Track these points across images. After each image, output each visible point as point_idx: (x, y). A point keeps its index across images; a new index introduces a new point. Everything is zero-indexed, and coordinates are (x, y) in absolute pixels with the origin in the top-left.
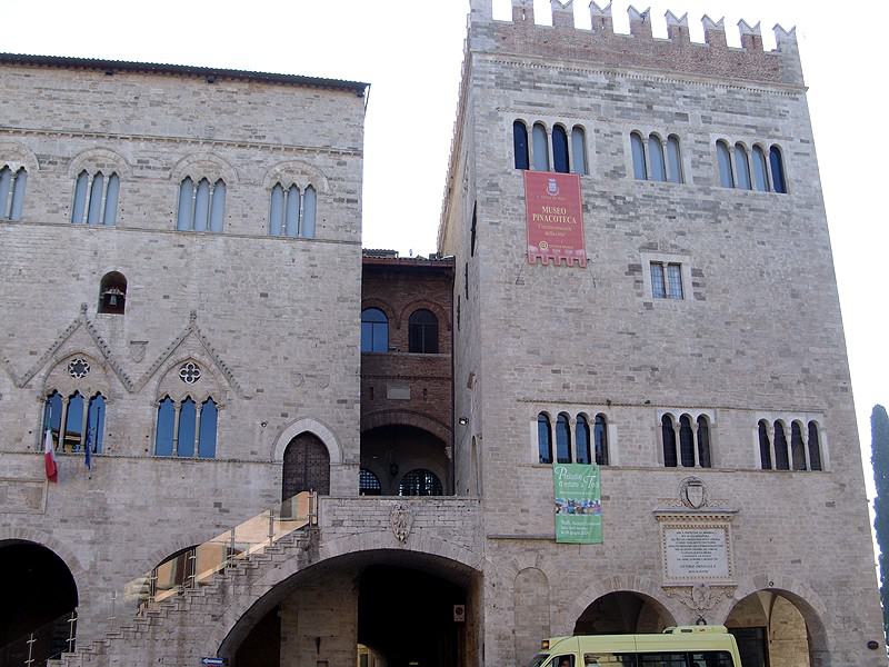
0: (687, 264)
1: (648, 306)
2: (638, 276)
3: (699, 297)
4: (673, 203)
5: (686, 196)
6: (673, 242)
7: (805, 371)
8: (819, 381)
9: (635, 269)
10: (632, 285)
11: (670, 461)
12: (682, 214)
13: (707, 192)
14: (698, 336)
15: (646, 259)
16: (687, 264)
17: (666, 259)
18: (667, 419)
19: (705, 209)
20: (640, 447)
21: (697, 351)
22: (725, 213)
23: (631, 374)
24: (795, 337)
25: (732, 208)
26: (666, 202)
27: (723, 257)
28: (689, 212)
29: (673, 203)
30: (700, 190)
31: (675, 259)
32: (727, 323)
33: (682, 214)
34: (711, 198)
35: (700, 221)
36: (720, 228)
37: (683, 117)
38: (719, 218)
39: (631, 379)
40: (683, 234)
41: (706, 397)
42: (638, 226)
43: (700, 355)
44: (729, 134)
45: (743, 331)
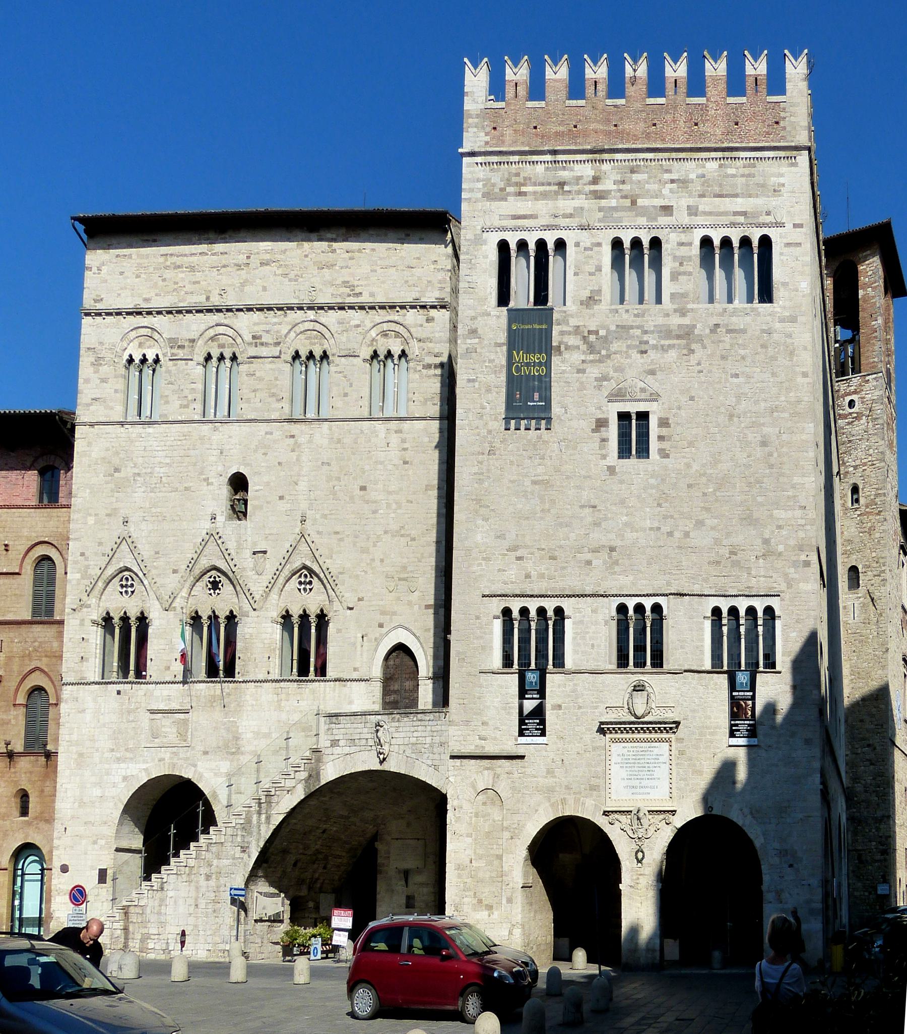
0: (654, 413)
1: (611, 470)
2: (603, 433)
3: (664, 454)
4: (646, 332)
5: (660, 321)
6: (642, 385)
7: (766, 542)
8: (780, 554)
9: (601, 424)
10: (597, 445)
11: (622, 661)
12: (655, 347)
13: (683, 312)
14: (659, 505)
15: (612, 411)
16: (654, 413)
17: (633, 408)
18: (622, 609)
19: (678, 337)
20: (593, 645)
21: (656, 525)
22: (700, 340)
23: (589, 556)
24: (759, 499)
25: (707, 331)
26: (638, 332)
27: (692, 399)
28: (663, 342)
29: (646, 332)
30: (675, 311)
31: (642, 407)
32: (690, 486)
33: (655, 347)
34: (686, 321)
35: (673, 354)
36: (694, 359)
37: (667, 210)
38: (693, 346)
39: (589, 563)
40: (652, 372)
41: (660, 585)
42: (607, 368)
43: (659, 529)
44: (714, 226)
45: (705, 494)
